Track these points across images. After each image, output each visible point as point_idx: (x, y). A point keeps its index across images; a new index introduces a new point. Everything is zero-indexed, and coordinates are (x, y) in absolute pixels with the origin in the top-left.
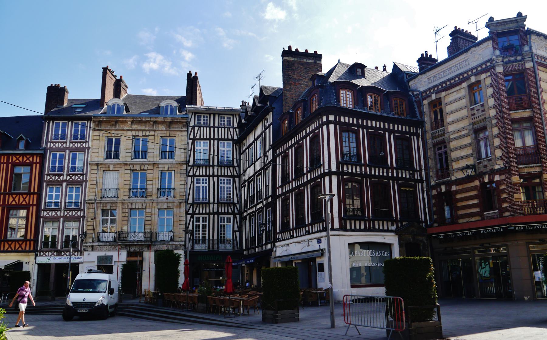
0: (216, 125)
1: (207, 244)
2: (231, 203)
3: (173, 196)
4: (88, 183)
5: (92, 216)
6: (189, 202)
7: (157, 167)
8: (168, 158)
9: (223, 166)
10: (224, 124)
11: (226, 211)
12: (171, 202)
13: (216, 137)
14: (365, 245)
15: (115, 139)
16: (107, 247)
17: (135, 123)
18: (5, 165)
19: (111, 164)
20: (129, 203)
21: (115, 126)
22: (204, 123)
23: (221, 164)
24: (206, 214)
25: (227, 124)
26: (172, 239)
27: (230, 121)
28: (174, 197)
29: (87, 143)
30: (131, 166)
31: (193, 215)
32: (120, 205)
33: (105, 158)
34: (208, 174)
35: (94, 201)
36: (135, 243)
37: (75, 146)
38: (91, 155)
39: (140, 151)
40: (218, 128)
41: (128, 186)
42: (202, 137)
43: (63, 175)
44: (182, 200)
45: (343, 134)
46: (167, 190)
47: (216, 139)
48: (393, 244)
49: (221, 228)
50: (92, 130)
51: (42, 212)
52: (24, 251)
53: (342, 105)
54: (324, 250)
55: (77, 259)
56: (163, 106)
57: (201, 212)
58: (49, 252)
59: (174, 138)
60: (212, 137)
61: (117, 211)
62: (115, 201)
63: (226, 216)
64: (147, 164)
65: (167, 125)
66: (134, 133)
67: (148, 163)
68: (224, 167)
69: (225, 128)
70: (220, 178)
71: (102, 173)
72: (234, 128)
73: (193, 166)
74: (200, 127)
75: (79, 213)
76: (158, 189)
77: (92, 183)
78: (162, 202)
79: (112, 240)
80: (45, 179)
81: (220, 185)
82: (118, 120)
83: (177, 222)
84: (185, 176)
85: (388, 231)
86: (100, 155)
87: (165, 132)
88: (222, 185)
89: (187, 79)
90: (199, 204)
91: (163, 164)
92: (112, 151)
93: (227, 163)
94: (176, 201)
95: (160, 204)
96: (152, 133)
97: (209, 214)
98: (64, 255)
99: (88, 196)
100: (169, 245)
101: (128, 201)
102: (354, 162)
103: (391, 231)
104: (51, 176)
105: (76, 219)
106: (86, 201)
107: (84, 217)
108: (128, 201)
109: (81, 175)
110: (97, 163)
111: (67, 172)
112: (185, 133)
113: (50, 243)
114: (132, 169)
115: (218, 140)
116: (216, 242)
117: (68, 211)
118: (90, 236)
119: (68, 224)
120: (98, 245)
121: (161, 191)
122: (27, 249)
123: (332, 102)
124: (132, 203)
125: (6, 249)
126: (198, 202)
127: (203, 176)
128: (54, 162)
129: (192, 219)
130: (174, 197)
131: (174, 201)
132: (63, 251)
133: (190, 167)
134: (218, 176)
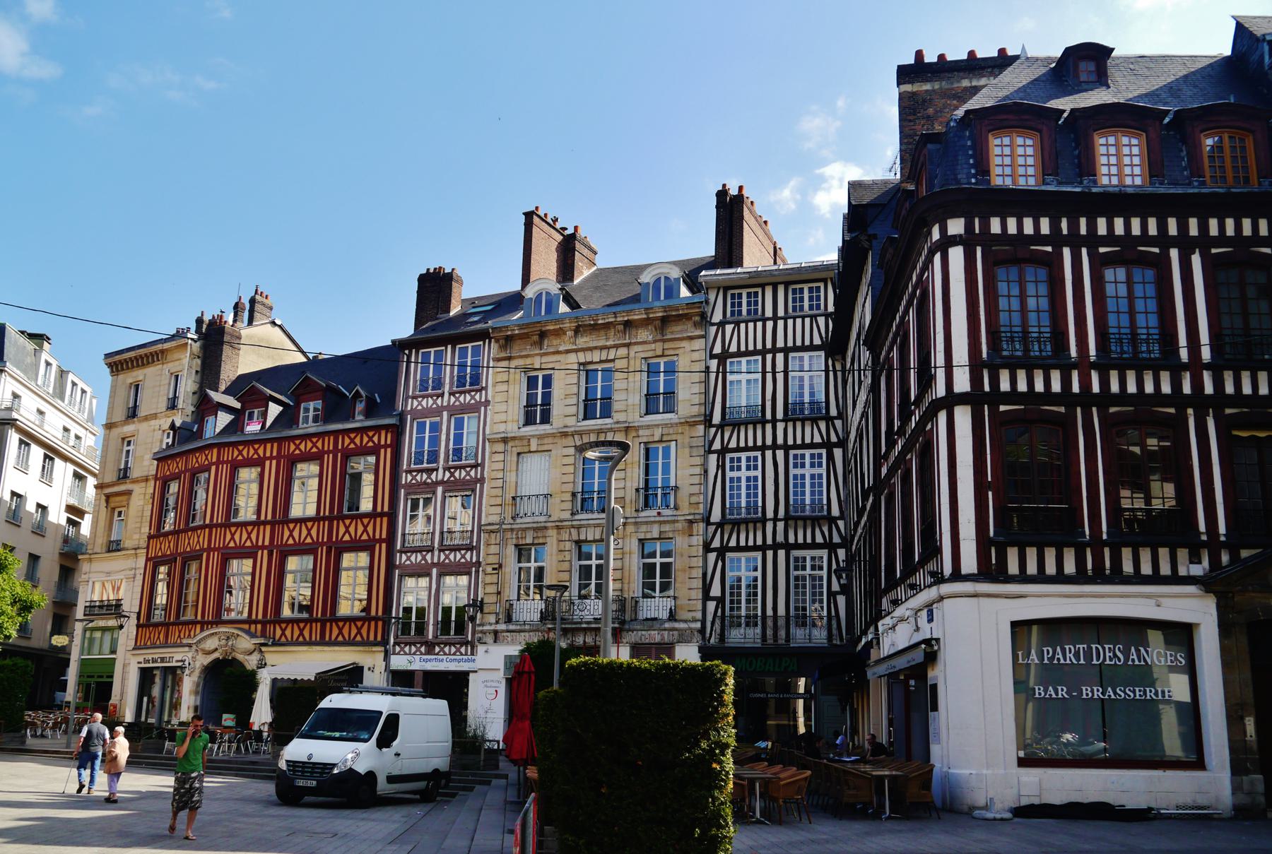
0: (781, 313)
2: (823, 518)
3: (672, 506)
6: (712, 520)
7: (634, 434)
8: (661, 411)
9: (798, 419)
10: (802, 308)
11: (809, 540)
12: (668, 522)
13: (780, 344)
14: (1055, 628)
15: (544, 376)
16: (527, 634)
17: (585, 331)
18: (331, 455)
19: (533, 436)
20: (573, 527)
21: (540, 344)
22: (749, 312)
23: (794, 415)
24: (755, 548)
25: (811, 307)
26: (672, 616)
27: (818, 298)
28: (676, 508)
29: (484, 392)
30: (576, 436)
32: (552, 533)
33: (522, 422)
34: (759, 443)
35: (498, 527)
36: (584, 626)
37: (460, 401)
38: (492, 420)
39: (596, 400)
40: (785, 319)
41: (570, 488)
42: (743, 348)
43: (437, 470)
44: (694, 514)
45: (1001, 272)
46: (660, 491)
47: (781, 350)
48: (1198, 625)
49: (797, 586)
51: (398, 554)
52: (365, 643)
53: (997, 181)
54: (934, 642)
55: (465, 661)
56: (646, 281)
57: (743, 543)
58: (410, 644)
59: (675, 358)
60: (769, 345)
61: (547, 548)
62: (542, 525)
63: (808, 554)
64: (611, 430)
65: (656, 329)
66: (582, 357)
67: (613, 426)
68: (803, 421)
69: (803, 317)
70: (792, 452)
71: (515, 458)
73: (721, 427)
74: (737, 324)
75: (468, 556)
76: (637, 490)
77: (495, 484)
78: (646, 523)
79: (537, 617)
80: (403, 482)
81: (792, 471)
82: (544, 329)
83: (684, 571)
84: (702, 452)
85: (1175, 579)
86: (510, 418)
87: (653, 345)
88: (799, 471)
89: (717, 207)
90: (736, 524)
91: (648, 427)
92: (536, 405)
93: (812, 410)
94: (680, 518)
95: (643, 528)
96: (622, 352)
97: (763, 548)
98: (439, 652)
99: (486, 516)
100: (665, 630)
101: (570, 523)
102: (1036, 357)
103: (1189, 580)
104: (414, 474)
105: (462, 570)
106: (483, 528)
107: (478, 563)
108: (570, 523)
109: (472, 466)
110: (503, 435)
111: (444, 462)
112: (699, 344)
113: (413, 626)
115: (786, 351)
116: (781, 622)
119: (449, 580)
120: (508, 631)
121: (647, 496)
122: (372, 638)
123: (959, 177)
124: (579, 528)
125: (333, 637)
126: (735, 519)
127: (746, 449)
128: (420, 441)
129: (720, 563)
130: (676, 508)
131: (676, 518)
132: (438, 644)
133: (713, 430)
134: (786, 448)
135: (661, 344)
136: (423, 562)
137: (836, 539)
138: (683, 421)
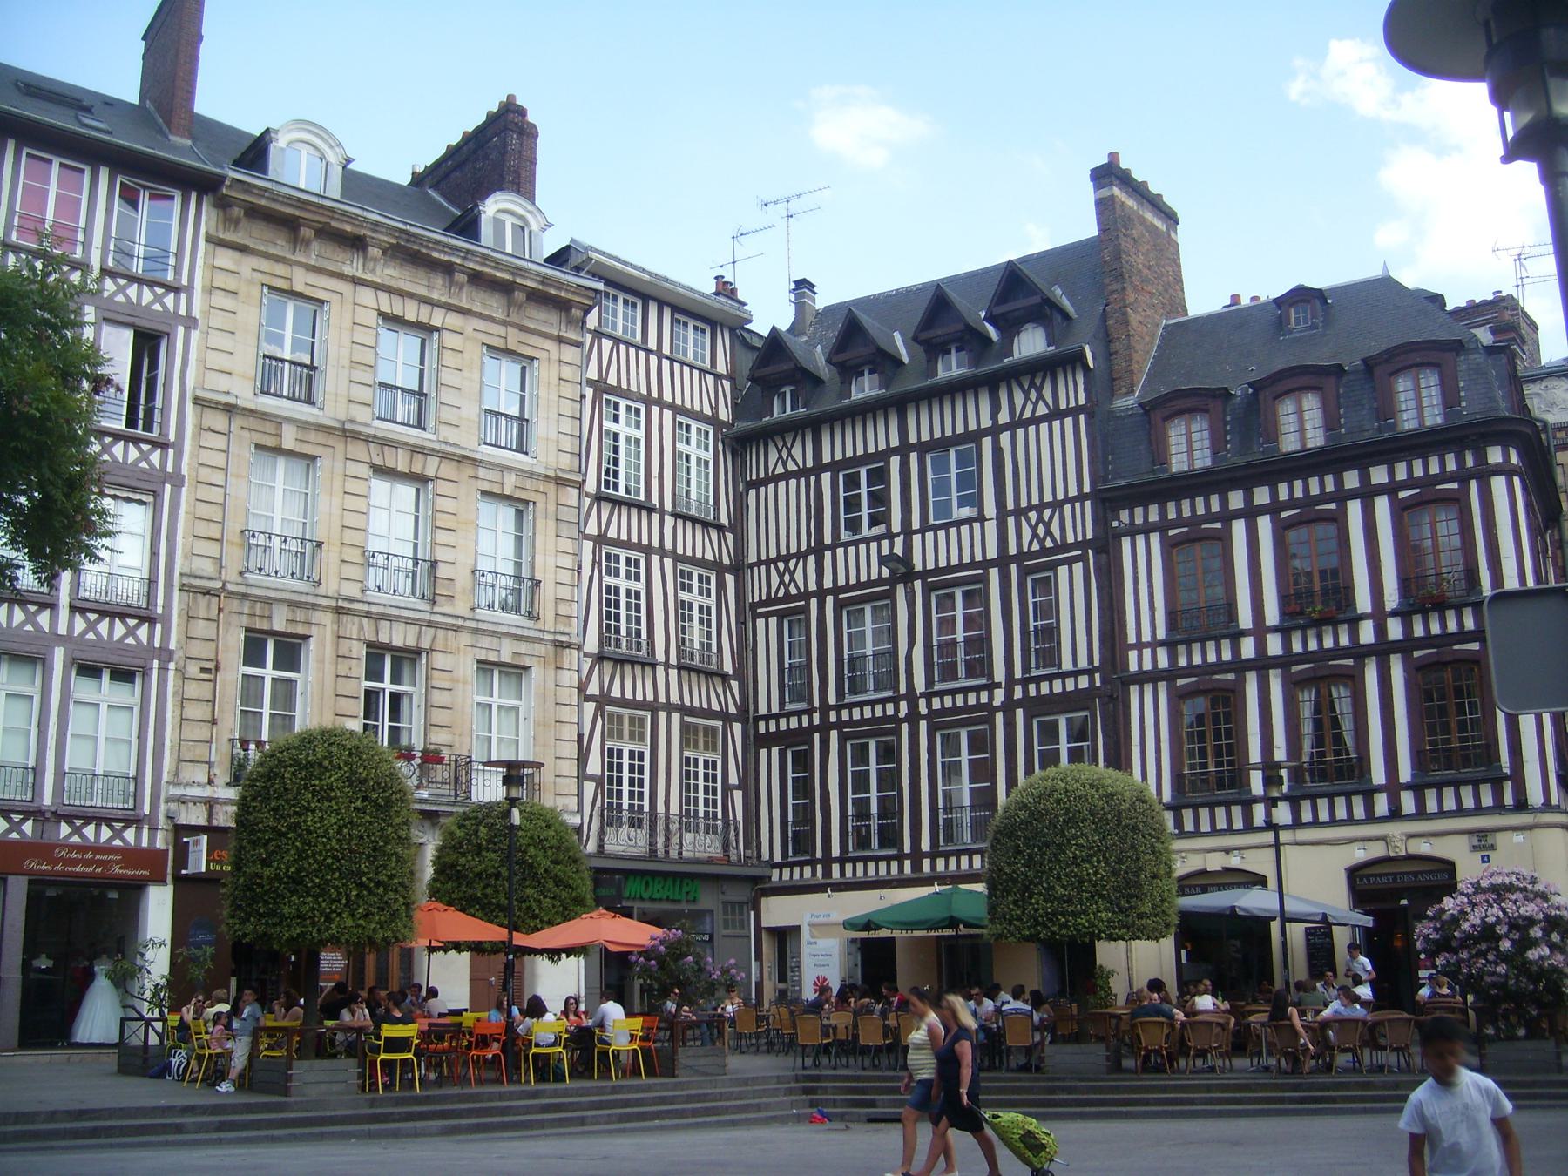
1: (646, 827)
4: (184, 489)
5: (203, 656)
29: (183, 296)
31: (603, 700)
32: (327, 618)
50: (209, 239)
72: (718, 377)
78: (493, 634)
109: (156, 444)
114: (378, 461)
116: (674, 827)
117: (132, 622)
118: (198, 751)
135: (516, 331)
136: (29, 627)
137: (732, 710)
138: (551, 473)
